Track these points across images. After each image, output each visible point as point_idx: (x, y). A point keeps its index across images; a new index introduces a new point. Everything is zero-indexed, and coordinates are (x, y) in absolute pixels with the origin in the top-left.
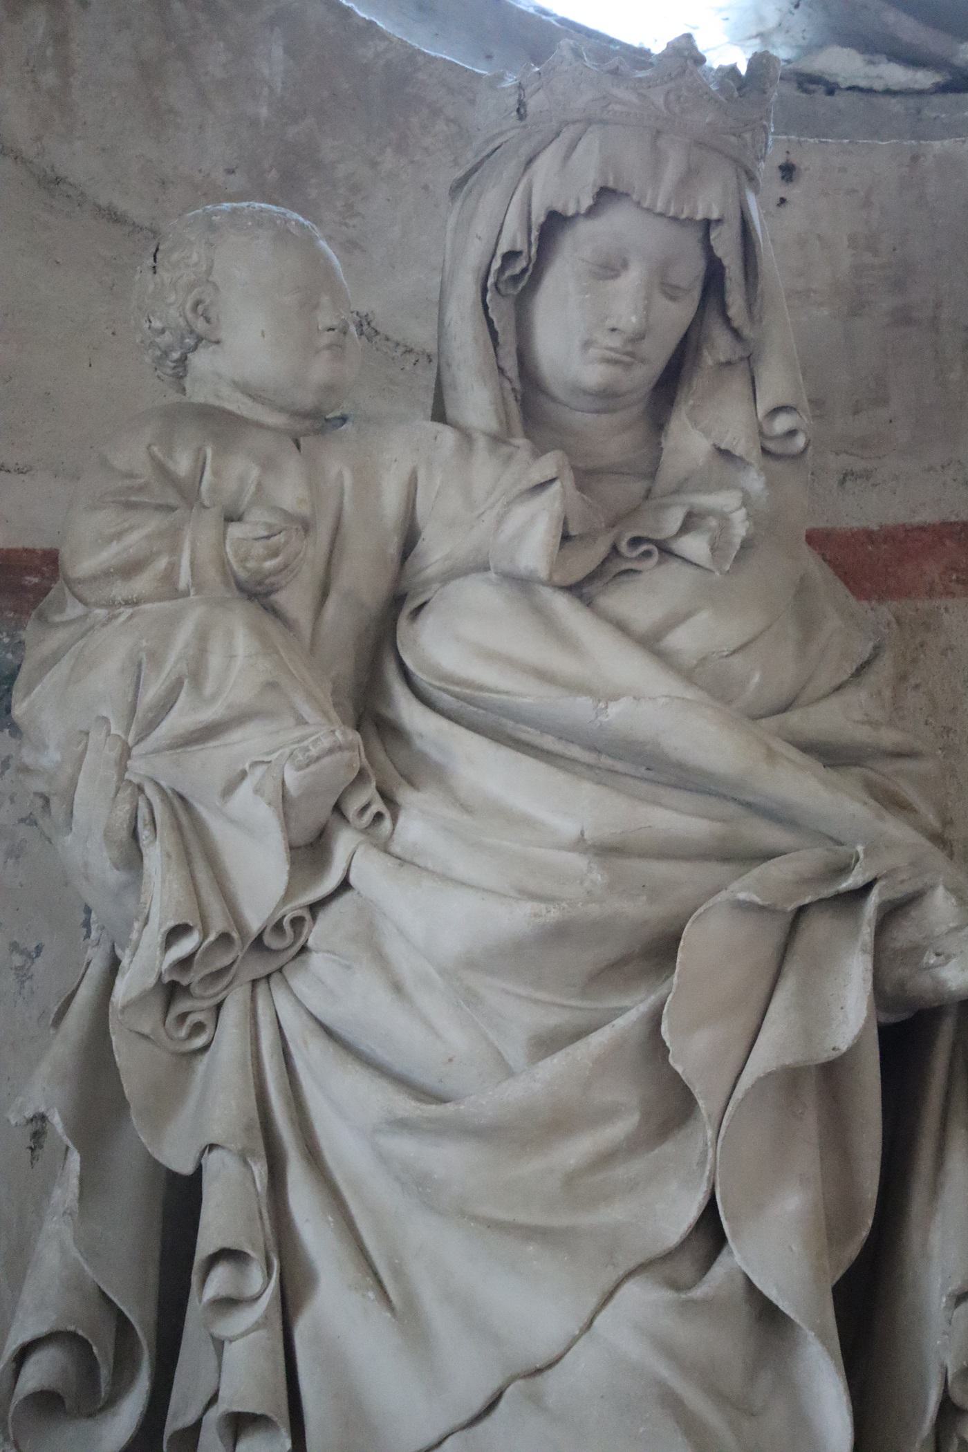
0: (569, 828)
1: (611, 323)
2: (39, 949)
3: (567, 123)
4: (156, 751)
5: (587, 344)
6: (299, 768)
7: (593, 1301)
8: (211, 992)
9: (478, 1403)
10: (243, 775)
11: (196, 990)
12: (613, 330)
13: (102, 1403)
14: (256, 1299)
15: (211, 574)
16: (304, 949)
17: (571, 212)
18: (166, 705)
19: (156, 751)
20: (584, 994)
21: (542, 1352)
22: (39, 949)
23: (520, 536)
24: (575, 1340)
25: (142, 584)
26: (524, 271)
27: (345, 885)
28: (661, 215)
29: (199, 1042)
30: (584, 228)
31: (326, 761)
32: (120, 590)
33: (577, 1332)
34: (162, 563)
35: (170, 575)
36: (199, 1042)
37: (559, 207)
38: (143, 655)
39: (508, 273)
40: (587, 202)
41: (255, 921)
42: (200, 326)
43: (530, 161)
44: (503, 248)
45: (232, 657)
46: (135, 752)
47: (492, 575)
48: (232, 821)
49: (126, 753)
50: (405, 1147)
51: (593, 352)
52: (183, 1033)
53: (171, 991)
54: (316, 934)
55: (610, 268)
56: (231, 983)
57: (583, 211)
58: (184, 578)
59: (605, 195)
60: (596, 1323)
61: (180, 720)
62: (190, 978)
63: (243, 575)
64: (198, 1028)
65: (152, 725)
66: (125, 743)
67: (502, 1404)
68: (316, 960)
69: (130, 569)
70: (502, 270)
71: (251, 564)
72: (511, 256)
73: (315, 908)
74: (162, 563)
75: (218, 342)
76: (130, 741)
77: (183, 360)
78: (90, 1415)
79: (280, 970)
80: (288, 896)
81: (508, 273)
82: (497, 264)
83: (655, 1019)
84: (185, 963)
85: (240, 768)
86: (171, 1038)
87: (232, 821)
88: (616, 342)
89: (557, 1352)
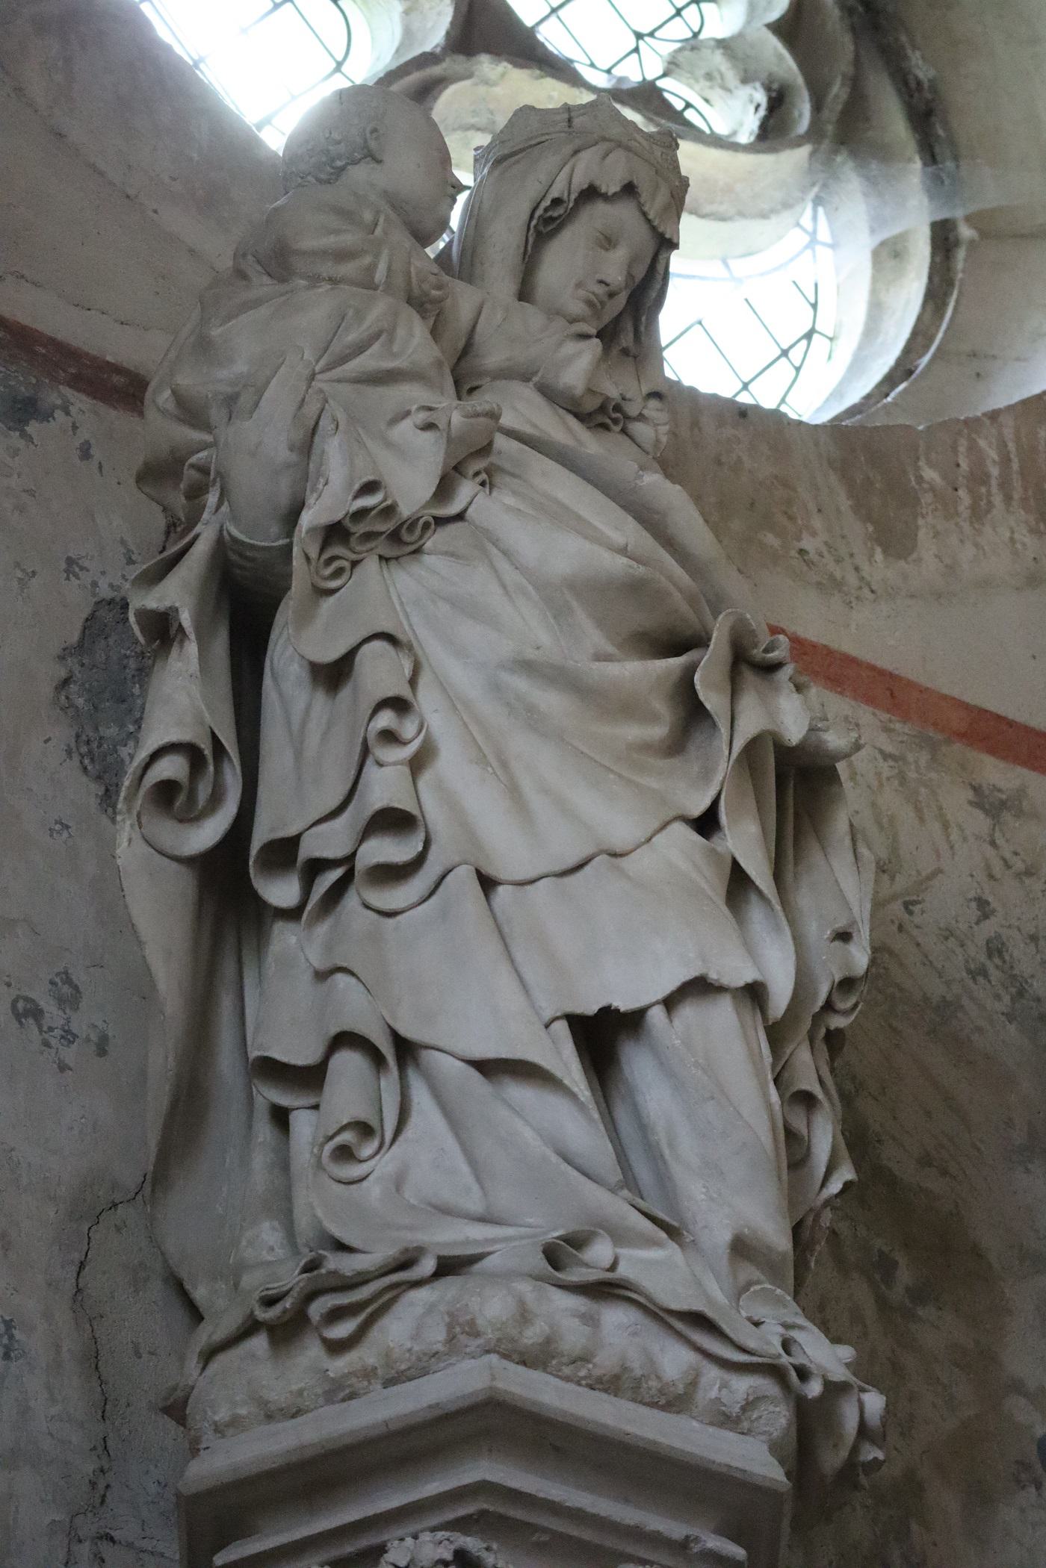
0: (618, 538)
1: (599, 277)
2: (34, 573)
3: (604, 139)
4: (339, 381)
5: (579, 285)
6: (466, 416)
7: (656, 825)
8: (358, 548)
9: (571, 861)
10: (408, 413)
11: (353, 540)
12: (601, 282)
13: (197, 813)
14: (405, 743)
15: (399, 281)
16: (418, 551)
17: (603, 190)
18: (360, 348)
19: (339, 381)
20: (620, 647)
21: (619, 846)
22: (34, 573)
23: (569, 360)
24: (638, 846)
25: (348, 269)
26: (560, 216)
27: (460, 517)
28: (649, 221)
29: (333, 584)
30: (600, 208)
31: (482, 419)
32: (327, 269)
33: (643, 840)
34: (367, 260)
35: (371, 269)
36: (333, 584)
37: (597, 183)
38: (351, 313)
39: (549, 214)
40: (614, 188)
41: (405, 511)
42: (373, 144)
43: (576, 152)
44: (554, 193)
45: (411, 335)
46: (319, 377)
47: (531, 384)
48: (389, 444)
49: (312, 377)
50: (520, 684)
51: (581, 292)
52: (328, 571)
53: (334, 533)
54: (435, 540)
55: (608, 242)
56: (372, 549)
57: (610, 194)
58: (380, 275)
59: (629, 190)
60: (654, 840)
61: (368, 361)
62: (360, 529)
63: (416, 292)
64: (338, 573)
65: (344, 360)
66: (314, 370)
67: (587, 869)
68: (427, 559)
69: (342, 255)
70: (546, 210)
71: (426, 286)
72: (557, 202)
73: (441, 521)
74: (367, 260)
75: (379, 162)
76: (317, 369)
77: (343, 169)
78: (181, 821)
79: (397, 558)
80: (424, 507)
81: (549, 214)
82: (547, 203)
83: (690, 671)
84: (360, 514)
85: (408, 408)
86: (317, 573)
87: (389, 444)
88: (600, 290)
89: (630, 847)
